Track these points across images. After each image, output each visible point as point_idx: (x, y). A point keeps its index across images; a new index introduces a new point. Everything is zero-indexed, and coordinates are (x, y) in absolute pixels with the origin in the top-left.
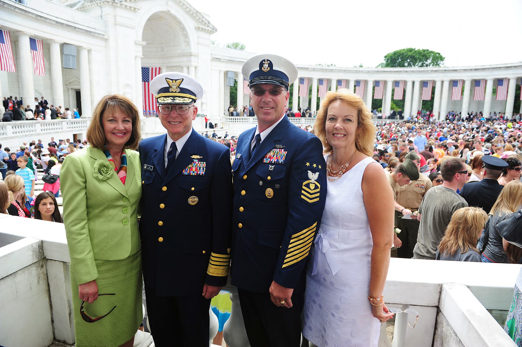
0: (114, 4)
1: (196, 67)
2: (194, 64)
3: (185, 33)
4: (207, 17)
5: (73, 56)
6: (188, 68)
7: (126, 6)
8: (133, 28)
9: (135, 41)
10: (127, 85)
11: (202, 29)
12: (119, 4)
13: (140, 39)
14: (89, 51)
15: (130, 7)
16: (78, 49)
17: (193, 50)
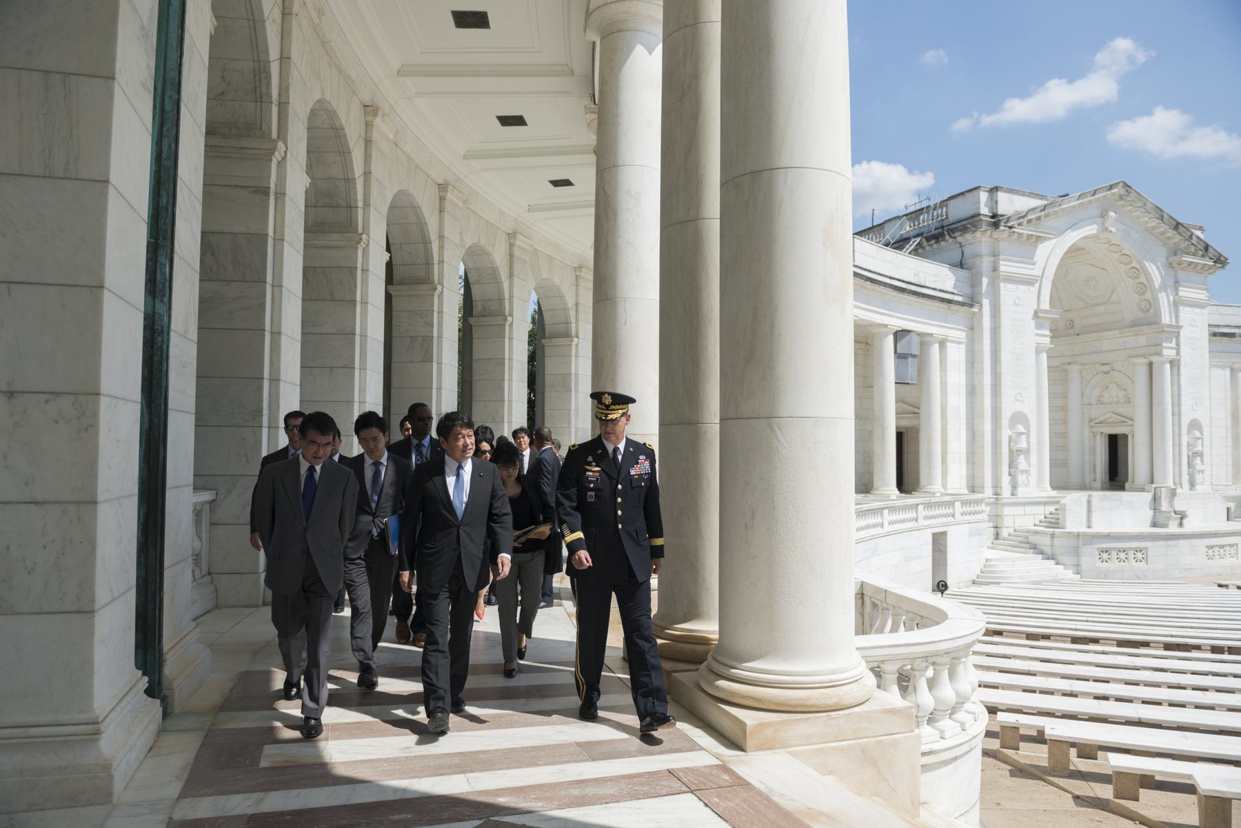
0: (996, 234)
1: (1171, 362)
2: (1169, 353)
3: (1142, 279)
4: (1198, 233)
5: (914, 356)
6: (1151, 365)
7: (1020, 234)
8: (1029, 282)
9: (1036, 313)
10: (1019, 418)
11: (1190, 263)
12: (1006, 233)
13: (1045, 306)
14: (942, 344)
15: (1029, 237)
16: (925, 340)
17: (1166, 319)
